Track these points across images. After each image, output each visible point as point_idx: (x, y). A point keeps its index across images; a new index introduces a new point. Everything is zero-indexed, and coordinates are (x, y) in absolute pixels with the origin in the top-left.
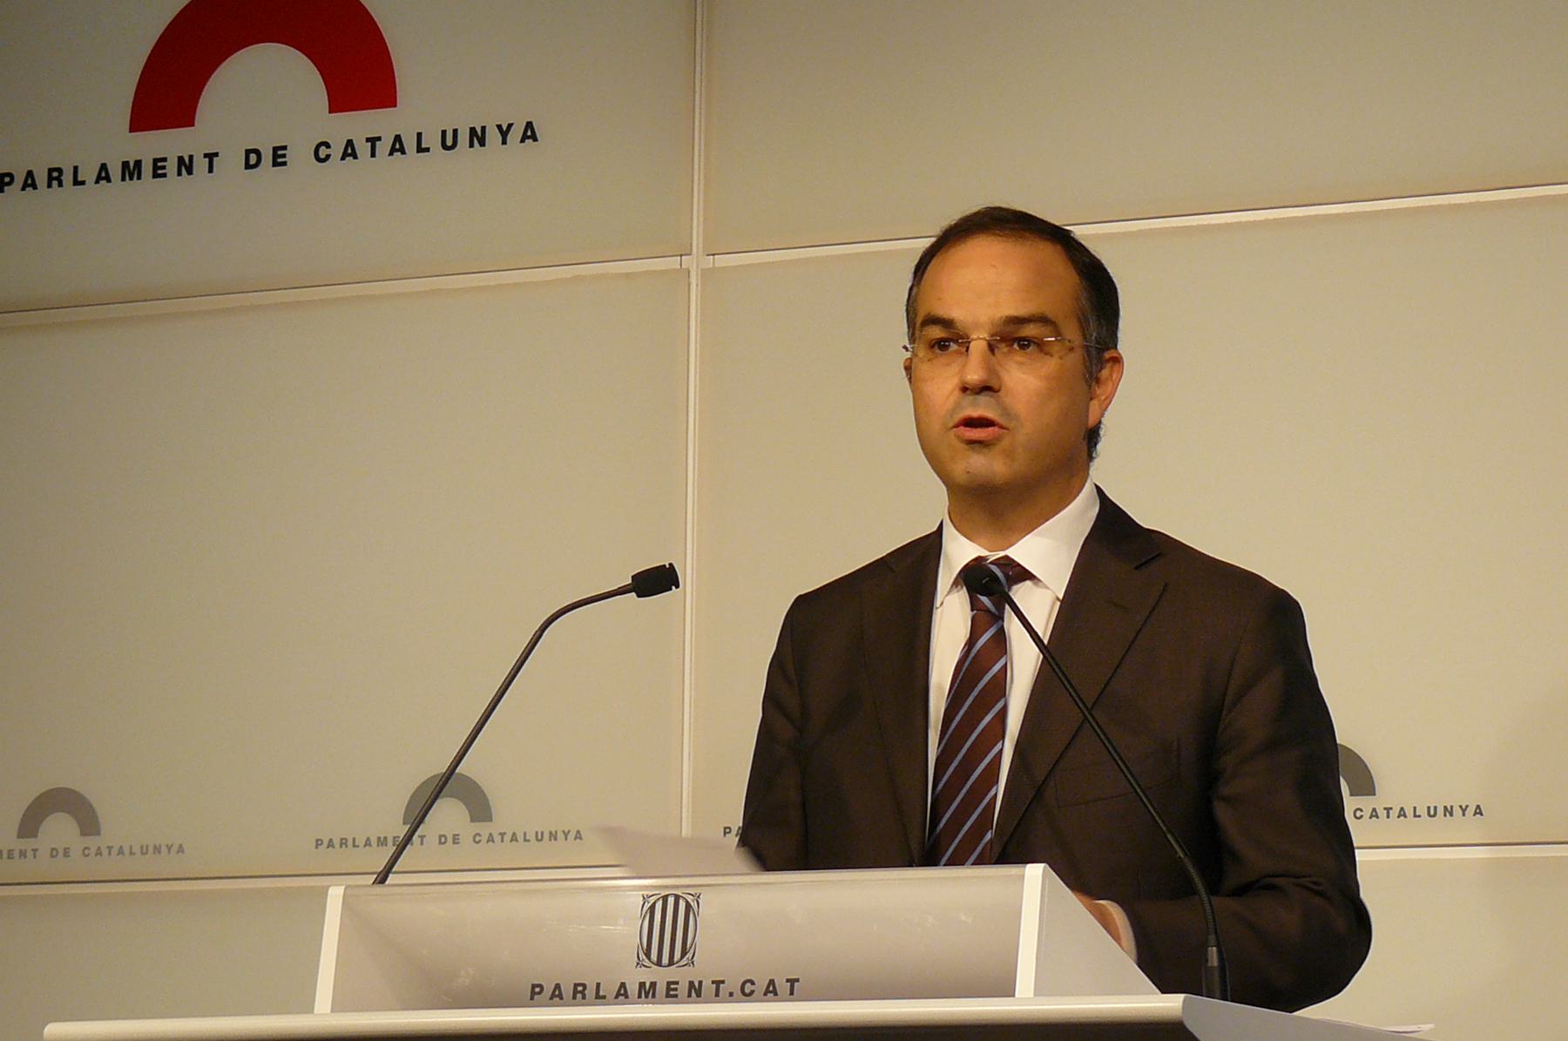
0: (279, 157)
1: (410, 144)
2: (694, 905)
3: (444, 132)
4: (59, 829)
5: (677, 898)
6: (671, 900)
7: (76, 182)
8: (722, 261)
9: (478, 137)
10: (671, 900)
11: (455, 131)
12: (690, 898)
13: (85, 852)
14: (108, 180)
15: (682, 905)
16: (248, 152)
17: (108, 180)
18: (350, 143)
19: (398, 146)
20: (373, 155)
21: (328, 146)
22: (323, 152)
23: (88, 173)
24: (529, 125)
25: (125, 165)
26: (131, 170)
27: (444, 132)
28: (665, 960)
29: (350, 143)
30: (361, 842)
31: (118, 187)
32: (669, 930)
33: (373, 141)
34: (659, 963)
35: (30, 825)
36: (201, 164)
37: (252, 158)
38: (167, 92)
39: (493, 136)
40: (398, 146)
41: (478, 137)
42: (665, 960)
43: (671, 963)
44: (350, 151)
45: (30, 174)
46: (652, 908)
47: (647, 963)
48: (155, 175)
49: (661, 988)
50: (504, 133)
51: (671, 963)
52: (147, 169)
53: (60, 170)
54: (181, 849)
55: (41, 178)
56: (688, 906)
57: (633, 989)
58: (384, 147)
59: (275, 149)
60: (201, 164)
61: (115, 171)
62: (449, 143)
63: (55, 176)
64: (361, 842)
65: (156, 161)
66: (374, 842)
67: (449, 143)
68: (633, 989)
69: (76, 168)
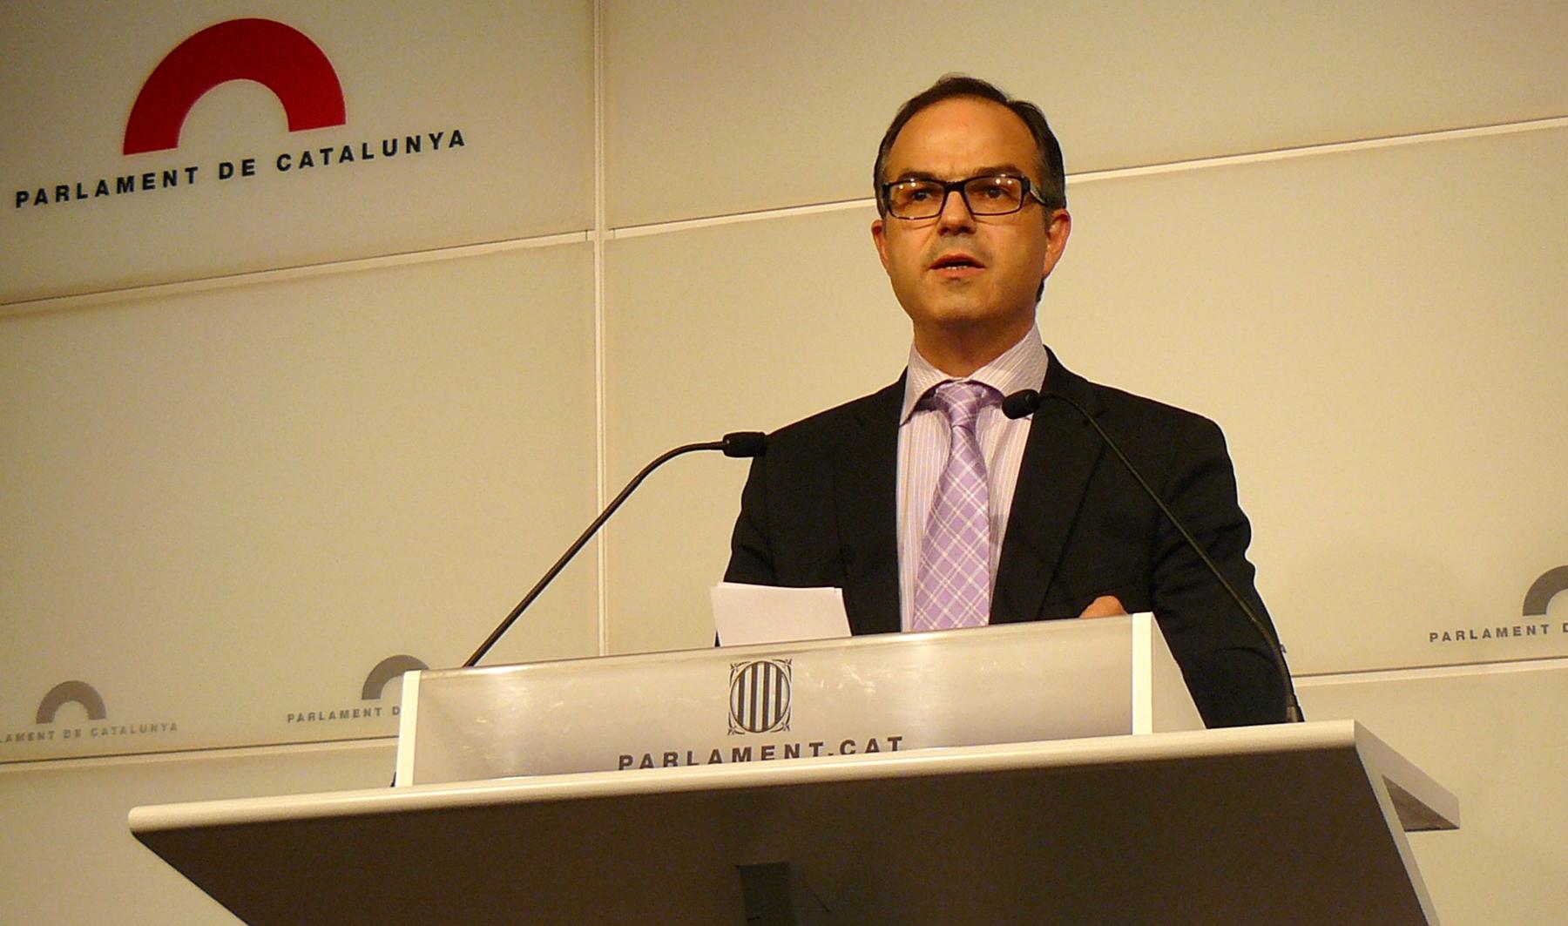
0: (247, 168)
1: (356, 152)
2: (785, 670)
3: (385, 143)
4: (71, 714)
5: (767, 665)
6: (761, 668)
7: (80, 196)
8: (620, 234)
9: (413, 144)
10: (761, 668)
11: (395, 141)
12: (780, 665)
13: (93, 732)
14: (106, 193)
15: (773, 671)
16: (222, 165)
17: (106, 193)
18: (306, 155)
19: (346, 155)
20: (326, 162)
21: (288, 157)
22: (284, 162)
23: (90, 188)
24: (457, 133)
25: (120, 180)
26: (125, 185)
27: (385, 143)
28: (759, 726)
29: (306, 155)
30: (326, 715)
31: (115, 199)
32: (761, 694)
33: (326, 152)
34: (752, 729)
35: (46, 712)
36: (182, 177)
37: (225, 171)
38: (156, 118)
39: (426, 143)
40: (346, 155)
41: (413, 144)
42: (759, 726)
43: (765, 728)
44: (306, 160)
45: (41, 192)
46: (742, 676)
47: (739, 729)
48: (145, 187)
49: (756, 752)
50: (435, 141)
51: (765, 728)
52: (138, 183)
53: (66, 188)
54: (173, 728)
55: (51, 195)
56: (779, 672)
57: (726, 753)
58: (334, 156)
59: (245, 162)
60: (182, 177)
61: (112, 186)
62: (390, 150)
63: (62, 192)
64: (326, 715)
65: (145, 176)
66: (337, 715)
67: (389, 150)
68: (726, 753)
69: (79, 186)
